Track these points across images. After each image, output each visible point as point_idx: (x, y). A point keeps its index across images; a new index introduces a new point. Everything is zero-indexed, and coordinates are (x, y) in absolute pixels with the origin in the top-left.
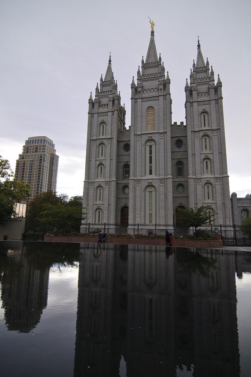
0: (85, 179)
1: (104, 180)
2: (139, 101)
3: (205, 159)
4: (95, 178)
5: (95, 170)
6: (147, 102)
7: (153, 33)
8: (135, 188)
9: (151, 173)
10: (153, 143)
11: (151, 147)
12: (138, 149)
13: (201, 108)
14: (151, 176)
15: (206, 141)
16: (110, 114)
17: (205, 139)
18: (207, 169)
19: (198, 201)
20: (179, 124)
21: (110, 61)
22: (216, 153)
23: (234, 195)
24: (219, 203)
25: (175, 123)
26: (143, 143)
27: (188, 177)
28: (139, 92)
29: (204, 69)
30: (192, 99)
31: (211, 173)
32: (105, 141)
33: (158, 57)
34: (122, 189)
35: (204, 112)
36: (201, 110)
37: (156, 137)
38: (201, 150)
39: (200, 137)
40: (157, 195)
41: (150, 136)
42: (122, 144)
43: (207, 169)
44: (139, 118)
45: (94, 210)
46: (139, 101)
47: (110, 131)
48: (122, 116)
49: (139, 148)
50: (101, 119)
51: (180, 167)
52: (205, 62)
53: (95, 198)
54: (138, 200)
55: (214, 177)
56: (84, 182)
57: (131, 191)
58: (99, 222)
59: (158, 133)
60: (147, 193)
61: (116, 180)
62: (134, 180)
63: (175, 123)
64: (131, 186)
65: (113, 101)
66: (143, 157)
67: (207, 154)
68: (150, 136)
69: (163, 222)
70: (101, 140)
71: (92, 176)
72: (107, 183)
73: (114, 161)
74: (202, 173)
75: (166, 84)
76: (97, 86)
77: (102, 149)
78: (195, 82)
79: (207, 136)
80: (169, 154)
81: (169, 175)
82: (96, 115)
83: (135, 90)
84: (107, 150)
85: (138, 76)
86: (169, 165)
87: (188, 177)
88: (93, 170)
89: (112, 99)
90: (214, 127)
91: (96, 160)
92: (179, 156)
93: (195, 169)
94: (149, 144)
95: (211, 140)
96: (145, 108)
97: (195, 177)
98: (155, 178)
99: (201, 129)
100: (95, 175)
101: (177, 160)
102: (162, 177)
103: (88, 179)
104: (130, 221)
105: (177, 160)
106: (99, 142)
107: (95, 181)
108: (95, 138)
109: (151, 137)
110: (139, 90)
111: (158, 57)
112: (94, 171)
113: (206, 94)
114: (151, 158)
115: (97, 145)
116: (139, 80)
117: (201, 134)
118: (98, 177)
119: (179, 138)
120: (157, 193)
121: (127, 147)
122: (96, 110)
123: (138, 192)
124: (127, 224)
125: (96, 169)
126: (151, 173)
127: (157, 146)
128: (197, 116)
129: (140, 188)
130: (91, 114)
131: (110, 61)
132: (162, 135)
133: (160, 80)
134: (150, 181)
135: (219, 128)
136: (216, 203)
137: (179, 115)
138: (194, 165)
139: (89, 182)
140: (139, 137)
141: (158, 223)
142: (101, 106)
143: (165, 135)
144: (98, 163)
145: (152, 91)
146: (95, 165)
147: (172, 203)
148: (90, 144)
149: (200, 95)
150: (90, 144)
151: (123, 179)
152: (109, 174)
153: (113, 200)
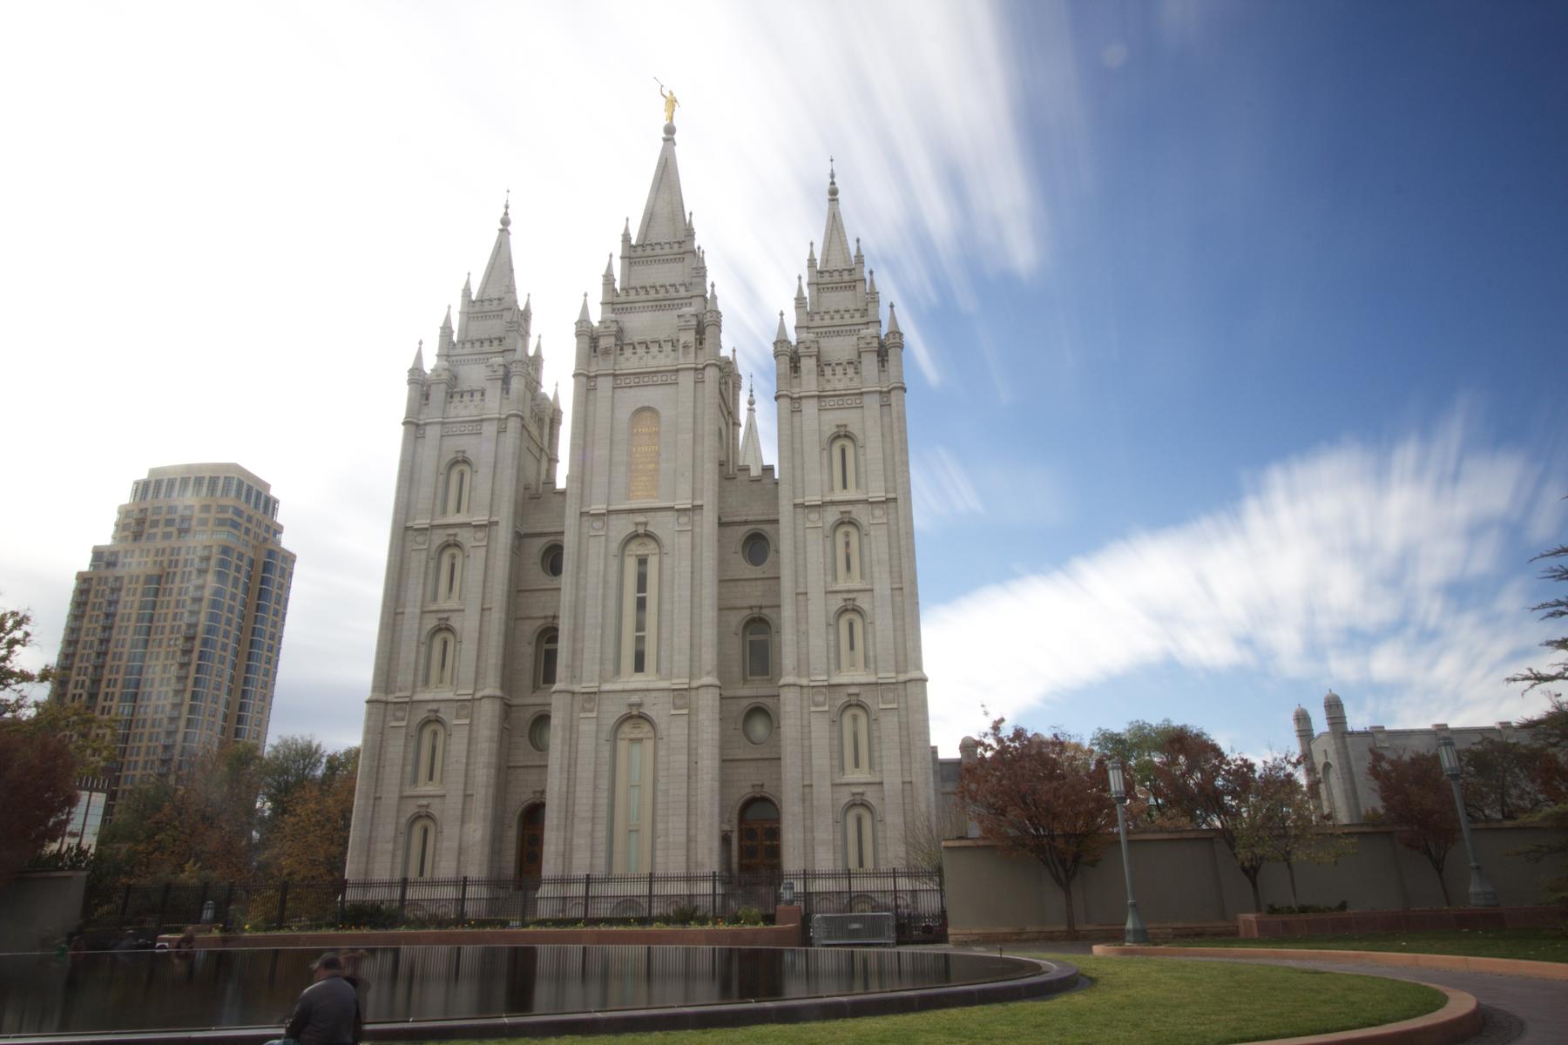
0: (375, 689)
1: (451, 695)
2: (605, 384)
3: (845, 610)
4: (414, 686)
5: (418, 652)
6: (632, 392)
7: (670, 131)
8: (571, 728)
9: (639, 666)
10: (649, 548)
11: (642, 562)
12: (593, 570)
13: (832, 420)
14: (639, 676)
15: (847, 544)
16: (490, 429)
17: (847, 534)
18: (852, 647)
19: (815, 776)
21: (505, 222)
22: (883, 586)
23: (934, 750)
24: (892, 781)
26: (614, 546)
27: (782, 682)
28: (606, 352)
29: (846, 277)
30: (800, 385)
31: (866, 665)
32: (464, 536)
34: (525, 729)
35: (843, 434)
36: (829, 430)
37: (662, 526)
38: (829, 579)
39: (828, 526)
40: (662, 753)
41: (641, 518)
42: (536, 547)
43: (852, 647)
44: (600, 452)
45: (403, 821)
46: (605, 384)
47: (490, 498)
48: (546, 431)
49: (595, 564)
50: (454, 445)
51: (755, 640)
52: (853, 252)
53: (409, 769)
54: (585, 772)
55: (872, 679)
56: (368, 702)
57: (559, 741)
58: (421, 873)
59: (671, 508)
60: (622, 746)
61: (498, 693)
62: (573, 693)
64: (556, 721)
66: (612, 603)
67: (849, 591)
68: (641, 518)
69: (677, 866)
70: (451, 531)
71: (404, 677)
72: (467, 705)
73: (497, 617)
74: (832, 667)
76: (448, 319)
77: (453, 566)
78: (814, 324)
79: (852, 523)
80: (709, 591)
81: (708, 673)
82: (433, 433)
84: (472, 572)
85: (605, 292)
86: (709, 633)
87: (782, 682)
88: (408, 652)
89: (501, 372)
90: (877, 493)
91: (423, 612)
92: (753, 595)
93: (806, 647)
94: (635, 549)
95: (866, 540)
96: (624, 414)
97: (804, 682)
98: (651, 686)
99: (828, 499)
100: (415, 675)
101: (748, 612)
102: (681, 682)
103: (387, 690)
104: (550, 867)
105: (748, 612)
106: (438, 538)
107: (417, 697)
108: (422, 522)
109: (646, 524)
110: (603, 343)
112: (413, 655)
113: (850, 371)
114: (641, 604)
115: (434, 548)
116: (609, 307)
117: (832, 515)
118: (426, 682)
120: (661, 745)
121: (553, 560)
122: (432, 414)
123: (586, 745)
124: (537, 882)
125: (423, 649)
126: (639, 666)
127: (667, 560)
128: (817, 450)
129: (594, 727)
130: (414, 427)
131: (505, 222)
132: (684, 519)
133: (685, 310)
134: (635, 699)
135: (891, 495)
136: (881, 783)
138: (802, 635)
139: (387, 703)
140: (598, 524)
141: (659, 872)
142: (457, 398)
143: (697, 518)
144: (431, 622)
146: (420, 629)
147: (717, 785)
148: (403, 546)
149: (828, 371)
150: (403, 546)
151: (535, 688)
152: (473, 673)
153: (483, 776)
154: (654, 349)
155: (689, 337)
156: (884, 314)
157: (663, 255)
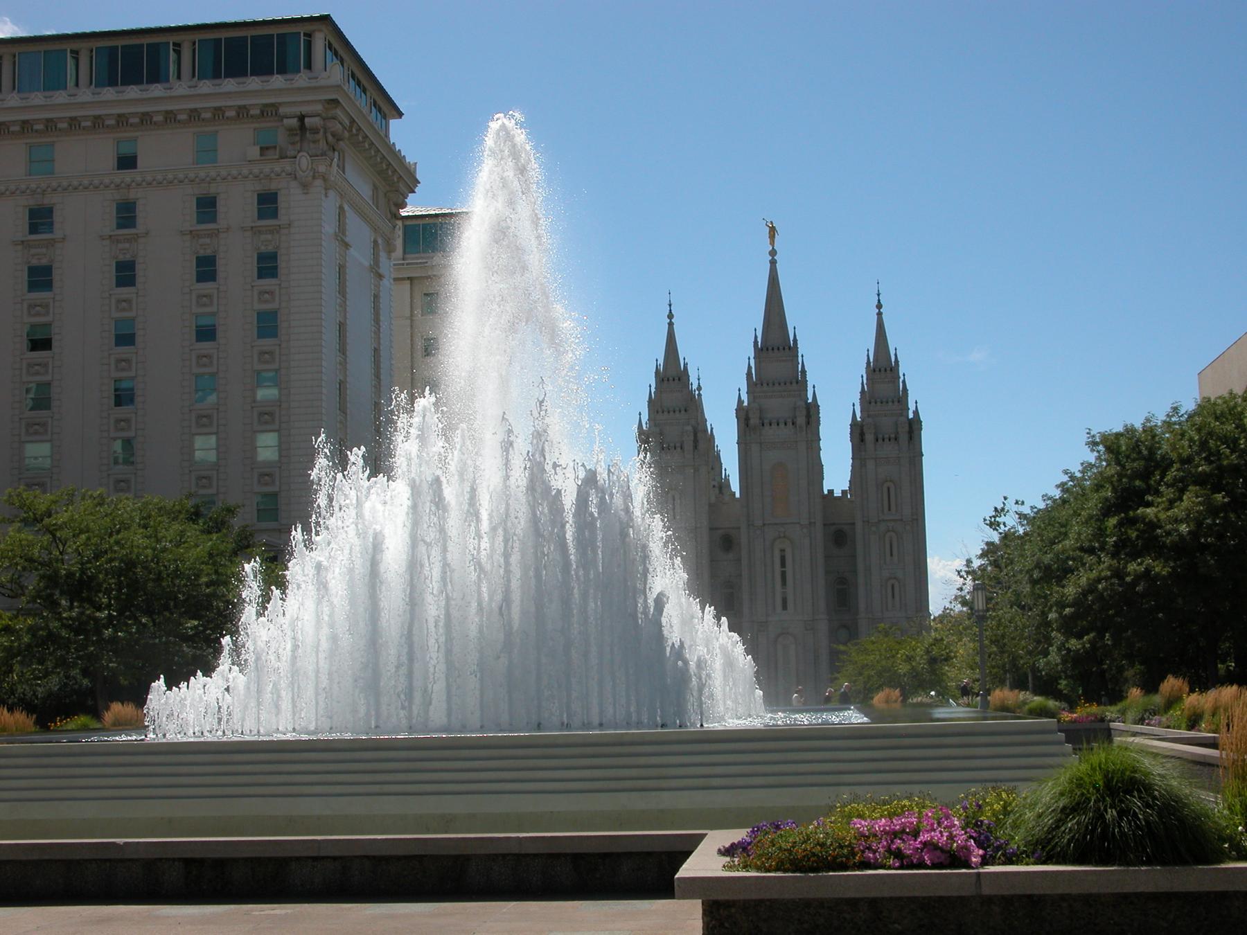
7: (773, 253)
9: (785, 607)
11: (783, 551)
20: (838, 493)
25: (831, 492)
33: (791, 338)
63: (831, 492)
65: (696, 441)
75: (811, 413)
83: (743, 415)
110: (754, 421)
111: (791, 338)
119: (838, 528)
126: (785, 607)
137: (837, 474)
145: (782, 425)
149: (880, 441)
154: (782, 425)
155: (801, 420)
156: (912, 407)
157: (776, 352)
